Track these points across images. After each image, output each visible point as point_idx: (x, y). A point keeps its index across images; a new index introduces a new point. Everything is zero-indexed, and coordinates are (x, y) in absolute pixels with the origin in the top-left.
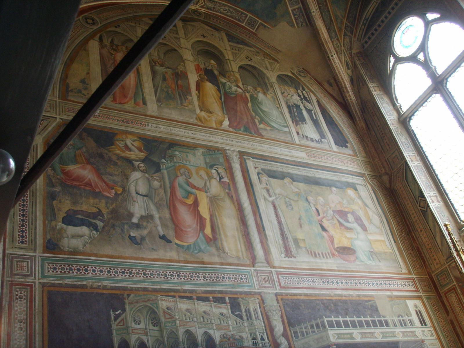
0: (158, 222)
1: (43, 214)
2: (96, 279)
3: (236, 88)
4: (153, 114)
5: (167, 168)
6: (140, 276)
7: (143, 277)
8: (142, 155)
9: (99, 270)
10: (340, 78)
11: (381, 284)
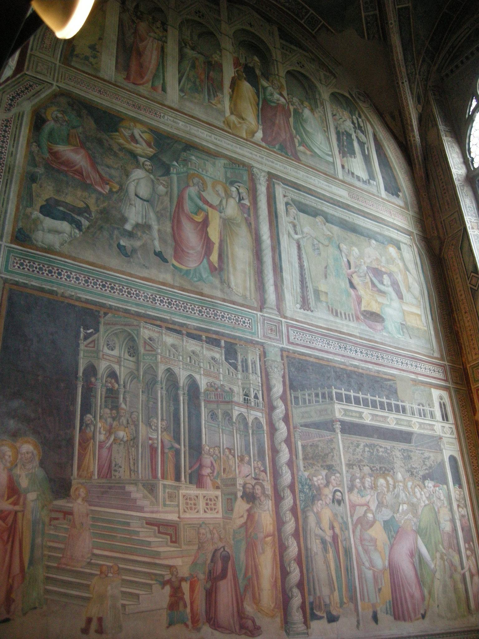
0: (155, 234)
1: (18, 197)
2: (69, 287)
3: (278, 96)
4: (172, 105)
5: (177, 174)
6: (123, 295)
7: (127, 296)
8: (150, 151)
9: (75, 277)
10: (407, 113)
11: (407, 364)
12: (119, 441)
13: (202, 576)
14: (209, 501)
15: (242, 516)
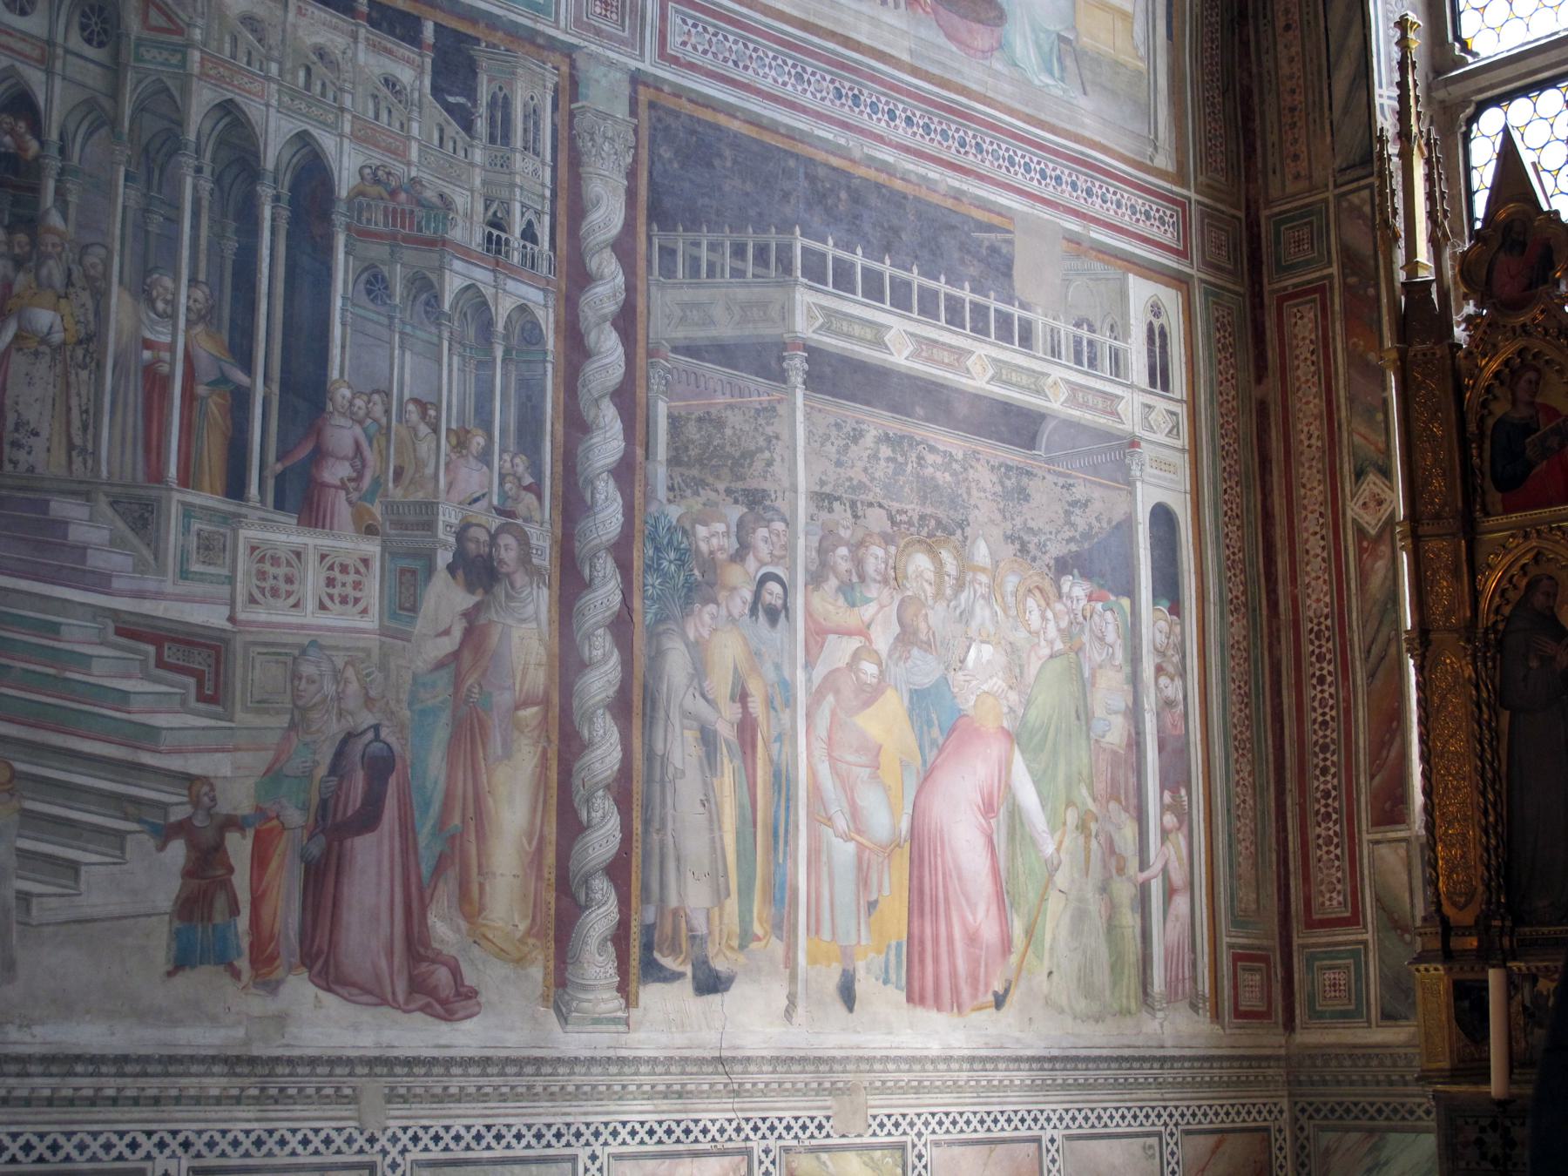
13: (294, 817)
14: (335, 569)
15: (447, 632)
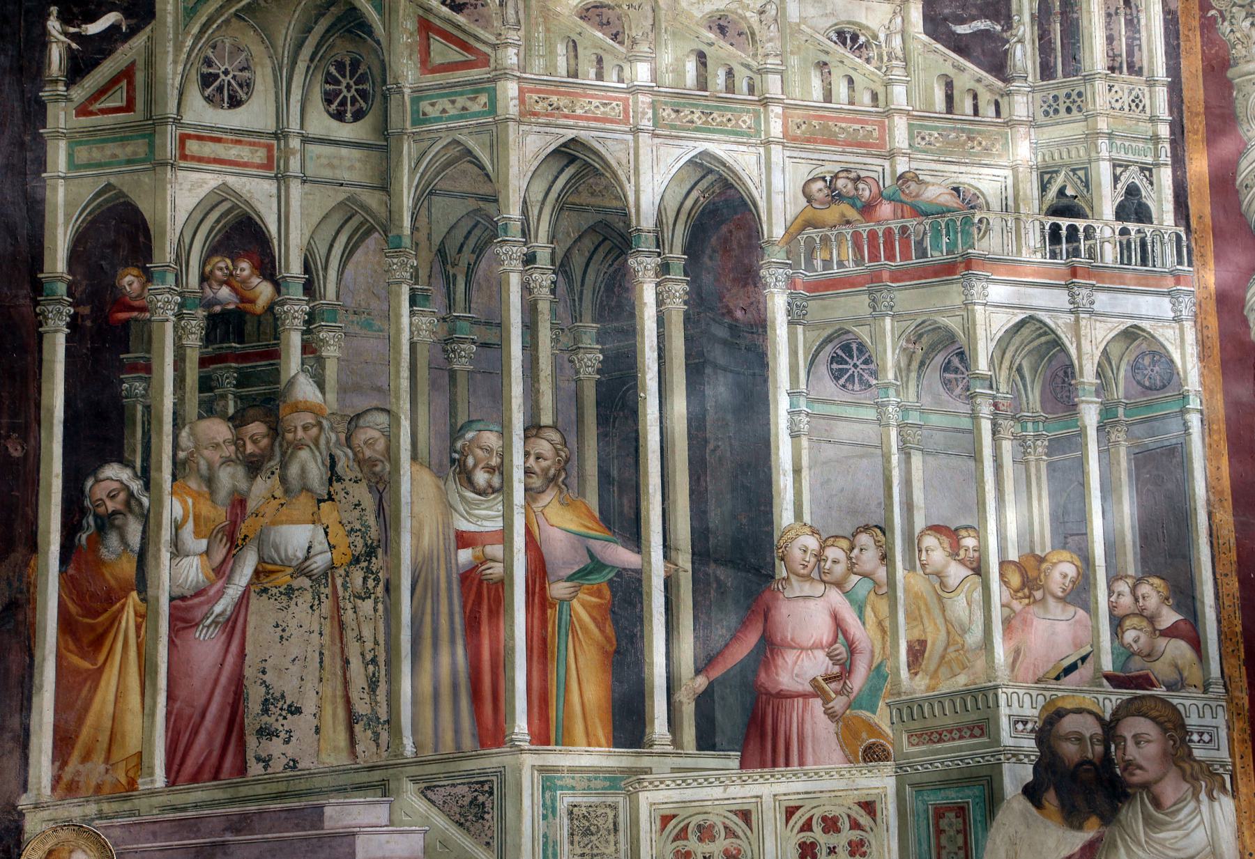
12: (284, 579)
